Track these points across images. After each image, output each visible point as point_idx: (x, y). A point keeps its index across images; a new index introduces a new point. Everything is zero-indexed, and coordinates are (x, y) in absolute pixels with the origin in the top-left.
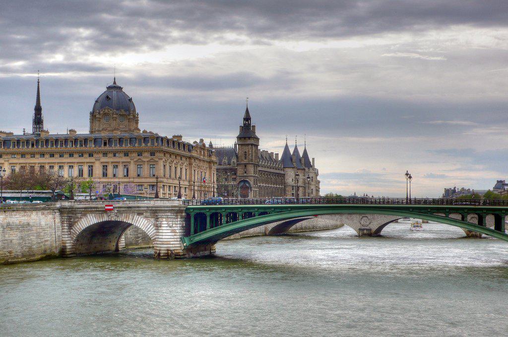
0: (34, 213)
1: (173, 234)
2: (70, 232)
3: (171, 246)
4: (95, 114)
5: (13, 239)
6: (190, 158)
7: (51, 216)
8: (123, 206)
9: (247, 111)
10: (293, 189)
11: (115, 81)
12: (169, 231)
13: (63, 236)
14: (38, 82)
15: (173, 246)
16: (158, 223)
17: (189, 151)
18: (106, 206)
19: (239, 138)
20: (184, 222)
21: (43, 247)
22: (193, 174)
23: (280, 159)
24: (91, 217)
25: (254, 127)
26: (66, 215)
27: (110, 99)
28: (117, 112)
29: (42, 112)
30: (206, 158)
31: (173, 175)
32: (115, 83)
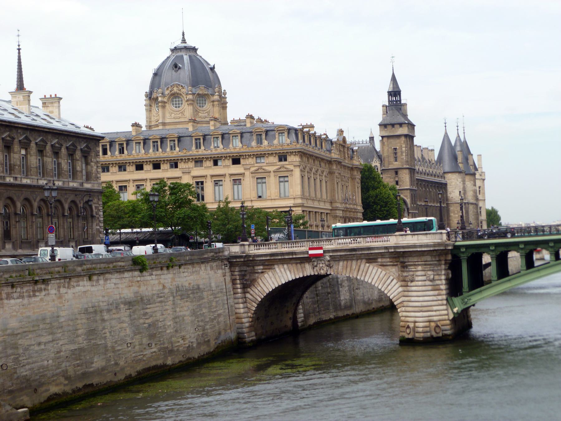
0: (203, 266)
1: (436, 292)
2: (245, 298)
3: (434, 313)
4: (154, 95)
5: (185, 316)
6: (330, 162)
7: (220, 272)
8: (339, 247)
9: (394, 79)
10: (461, 209)
11: (183, 38)
12: (430, 288)
13: (237, 306)
14: (19, 49)
15: (438, 313)
16: (405, 274)
18: (310, 249)
19: (383, 126)
20: (450, 272)
21: (217, 328)
22: (336, 190)
23: (436, 159)
24: (282, 270)
26: (237, 269)
27: (180, 68)
28: (194, 90)
31: (313, 195)
32: (184, 41)
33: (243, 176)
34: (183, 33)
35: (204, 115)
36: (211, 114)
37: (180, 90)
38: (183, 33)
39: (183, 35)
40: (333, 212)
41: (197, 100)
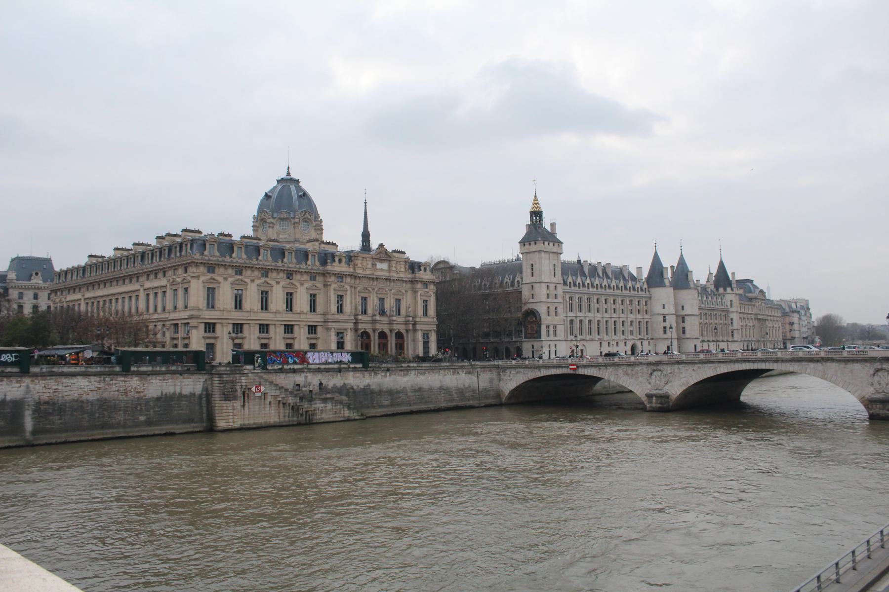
10: (665, 320)
17: (324, 263)
19: (523, 242)
23: (645, 274)
25: (553, 225)
30: (402, 275)
32: (288, 174)
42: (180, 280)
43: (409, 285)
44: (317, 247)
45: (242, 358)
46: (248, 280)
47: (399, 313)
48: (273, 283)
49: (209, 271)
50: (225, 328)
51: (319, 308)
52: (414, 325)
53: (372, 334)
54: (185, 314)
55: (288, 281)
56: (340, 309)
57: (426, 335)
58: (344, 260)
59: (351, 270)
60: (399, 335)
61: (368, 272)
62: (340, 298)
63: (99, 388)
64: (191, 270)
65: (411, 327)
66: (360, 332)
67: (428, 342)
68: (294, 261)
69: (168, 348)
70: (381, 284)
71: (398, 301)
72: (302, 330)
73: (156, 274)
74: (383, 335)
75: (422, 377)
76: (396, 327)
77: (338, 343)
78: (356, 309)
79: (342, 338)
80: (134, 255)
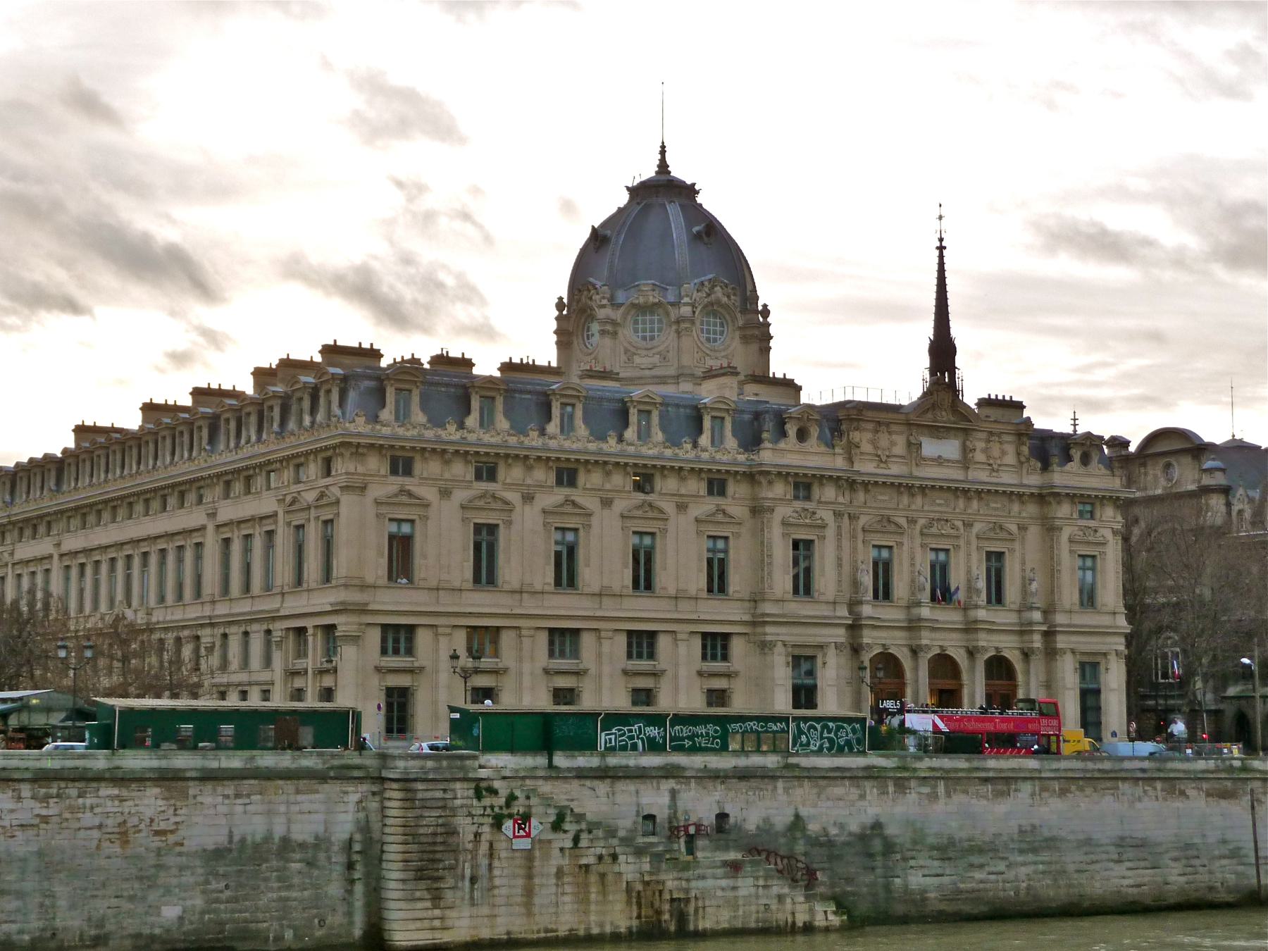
14: (941, 249)
17: (751, 442)
29: (959, 362)
30: (1008, 478)
32: (663, 166)
33: (276, 522)
34: (663, 147)
35: (650, 360)
36: (670, 355)
37: (591, 299)
38: (663, 147)
39: (663, 151)
40: (759, 630)
41: (636, 322)
42: (310, 497)
43: (1032, 509)
44: (732, 395)
45: (479, 728)
46: (513, 497)
47: (996, 595)
48: (590, 502)
49: (394, 471)
50: (443, 641)
51: (737, 581)
52: (1049, 635)
53: (907, 664)
54: (323, 600)
55: (641, 496)
56: (803, 585)
57: (1090, 668)
58: (814, 432)
59: (840, 462)
60: (999, 668)
61: (895, 469)
62: (802, 548)
63: (45, 819)
64: (342, 466)
65: (1037, 642)
66: (866, 658)
67: (1097, 692)
68: (658, 436)
69: (278, 701)
70: (939, 505)
71: (995, 560)
72: (682, 649)
73: (248, 479)
74: (944, 666)
75: (1056, 804)
76: (989, 643)
77: (797, 690)
78: (856, 584)
79: (811, 673)
80: (190, 424)
